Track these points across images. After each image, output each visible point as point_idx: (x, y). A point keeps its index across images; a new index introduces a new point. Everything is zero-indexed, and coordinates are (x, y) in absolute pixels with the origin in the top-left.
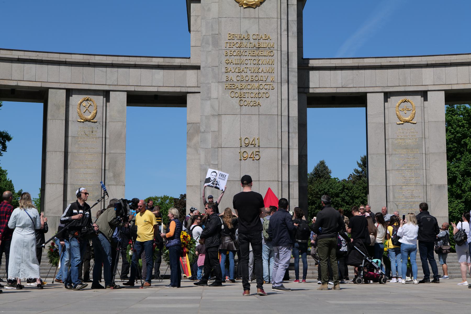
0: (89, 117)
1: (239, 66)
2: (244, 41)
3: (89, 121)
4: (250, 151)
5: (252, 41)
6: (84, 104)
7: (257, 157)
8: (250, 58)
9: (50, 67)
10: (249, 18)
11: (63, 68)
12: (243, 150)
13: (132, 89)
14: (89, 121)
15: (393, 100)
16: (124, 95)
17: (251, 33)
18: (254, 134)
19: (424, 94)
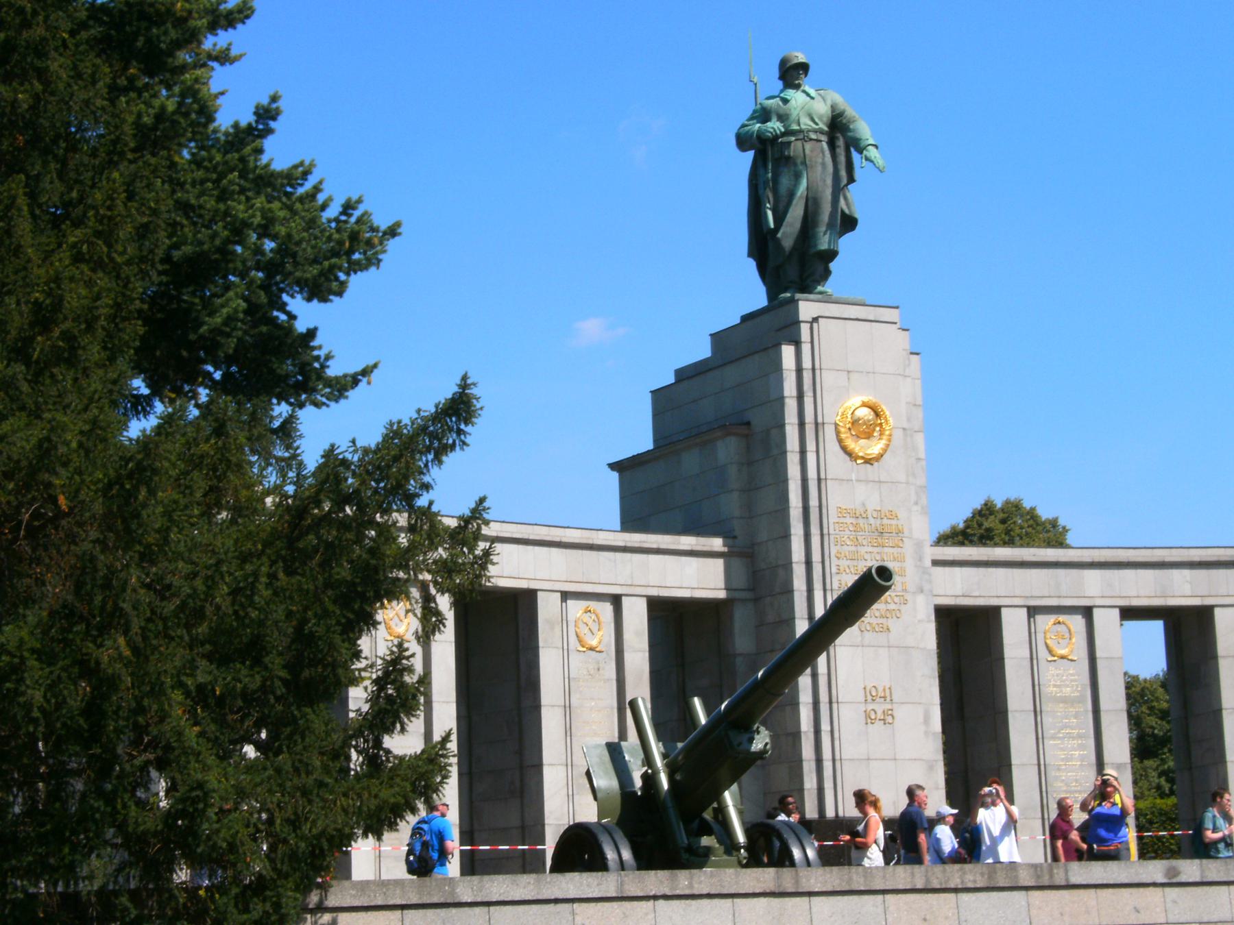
0: (594, 643)
1: (855, 563)
2: (861, 521)
3: (592, 649)
4: (880, 708)
5: (872, 521)
6: (586, 618)
7: (889, 719)
8: (870, 549)
9: (537, 549)
10: (867, 481)
11: (554, 550)
12: (870, 707)
13: (654, 592)
14: (592, 649)
15: (1040, 619)
16: (642, 606)
17: (870, 507)
18: (883, 681)
19: (1087, 612)
